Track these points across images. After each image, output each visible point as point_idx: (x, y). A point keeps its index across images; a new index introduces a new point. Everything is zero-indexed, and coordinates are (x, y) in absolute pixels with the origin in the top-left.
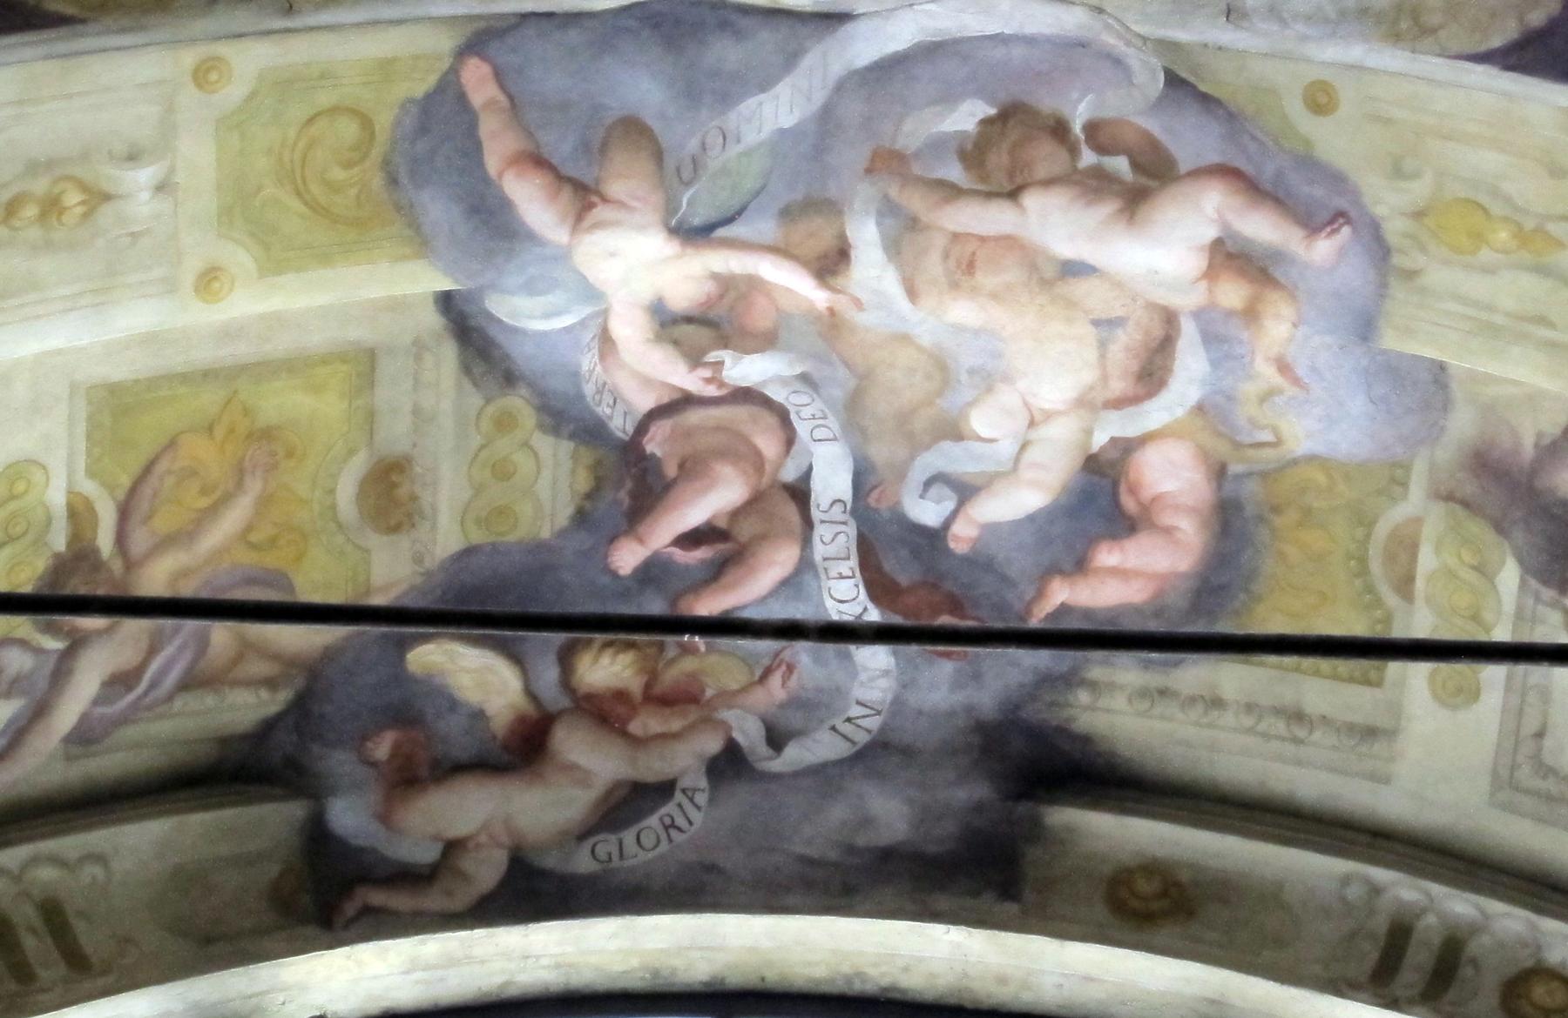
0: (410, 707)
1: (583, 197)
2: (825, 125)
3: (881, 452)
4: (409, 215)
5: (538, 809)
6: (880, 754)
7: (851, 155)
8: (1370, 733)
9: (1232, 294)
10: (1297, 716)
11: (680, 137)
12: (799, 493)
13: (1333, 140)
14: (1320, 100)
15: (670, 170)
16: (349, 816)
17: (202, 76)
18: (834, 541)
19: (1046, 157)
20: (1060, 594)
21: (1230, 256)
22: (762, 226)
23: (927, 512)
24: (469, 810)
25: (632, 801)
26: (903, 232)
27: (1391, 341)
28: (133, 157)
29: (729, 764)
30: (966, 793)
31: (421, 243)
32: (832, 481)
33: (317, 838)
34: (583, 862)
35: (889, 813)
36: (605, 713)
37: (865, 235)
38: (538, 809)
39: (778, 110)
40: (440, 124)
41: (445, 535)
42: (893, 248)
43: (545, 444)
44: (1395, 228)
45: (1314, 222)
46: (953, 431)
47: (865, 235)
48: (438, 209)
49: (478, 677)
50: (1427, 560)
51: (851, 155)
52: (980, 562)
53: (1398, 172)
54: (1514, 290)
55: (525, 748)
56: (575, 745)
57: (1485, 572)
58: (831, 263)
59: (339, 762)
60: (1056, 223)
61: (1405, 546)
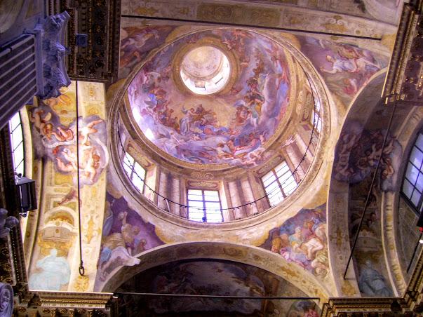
0: (45, 113)
1: (91, 128)
2: (97, 144)
3: (69, 147)
4: (90, 116)
5: (38, 124)
6: (44, 147)
7: (95, 146)
8: (51, 184)
9: (87, 174)
10: (51, 178)
11: (95, 134)
12: (65, 141)
13: (100, 181)
14: (103, 180)
15: (93, 134)
16: (36, 110)
17: (102, 103)
18: (62, 143)
19: (96, 160)
20: (59, 160)
21: (89, 174)
22: (89, 140)
23: (65, 150)
24: (37, 118)
25: (38, 130)
26: (89, 150)
27: (85, 186)
28: (95, 98)
29: (42, 136)
30: (42, 155)
31: (87, 117)
32: (66, 143)
33: (35, 108)
34: (34, 128)
35: (39, 149)
36: (45, 127)
37: (89, 147)
38: (38, 124)
39: (98, 141)
40: (98, 118)
41: (60, 116)
42: (87, 149)
43: (68, 123)
44: (94, 185)
45: (93, 180)
46: (72, 152)
47: (89, 147)
48: (90, 118)
49: (48, 117)
50: (65, 187)
51: (95, 146)
52: (61, 154)
53: (98, 185)
54: (90, 195)
55: (42, 121)
56: (43, 125)
57: (66, 192)
58: (86, 144)
59: (41, 108)
60: (91, 161)
61: (67, 186)
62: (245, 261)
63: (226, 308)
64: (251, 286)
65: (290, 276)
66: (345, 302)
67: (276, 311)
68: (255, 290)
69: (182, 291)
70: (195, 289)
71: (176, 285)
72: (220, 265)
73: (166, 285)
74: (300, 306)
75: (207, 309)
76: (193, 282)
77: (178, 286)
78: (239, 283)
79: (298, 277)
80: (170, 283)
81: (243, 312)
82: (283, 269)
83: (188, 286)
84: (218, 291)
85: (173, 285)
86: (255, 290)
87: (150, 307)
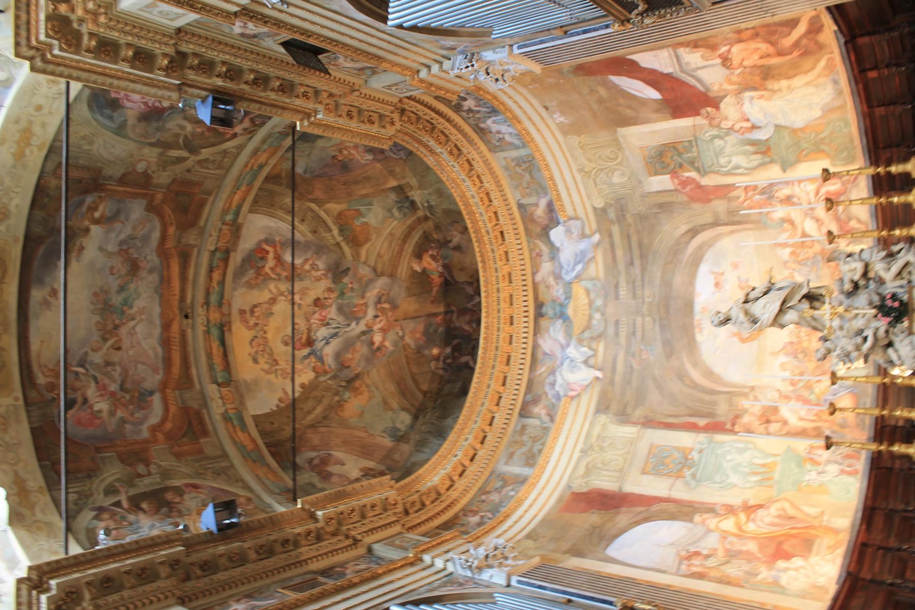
62: (16, 240)
63: (151, 271)
64: (87, 223)
65: (35, 141)
66: (24, 17)
67: (141, 167)
68: (97, 215)
69: (109, 369)
70: (105, 340)
71: (93, 385)
72: (37, 295)
73: (91, 407)
74: (111, 118)
75: (157, 310)
76: (88, 349)
77: (95, 379)
78: (82, 248)
79: (30, 122)
80: (85, 400)
81: (156, 235)
82: (19, 156)
83: (97, 358)
84: (107, 292)
85: (91, 392)
86: (97, 215)
87: (145, 434)
